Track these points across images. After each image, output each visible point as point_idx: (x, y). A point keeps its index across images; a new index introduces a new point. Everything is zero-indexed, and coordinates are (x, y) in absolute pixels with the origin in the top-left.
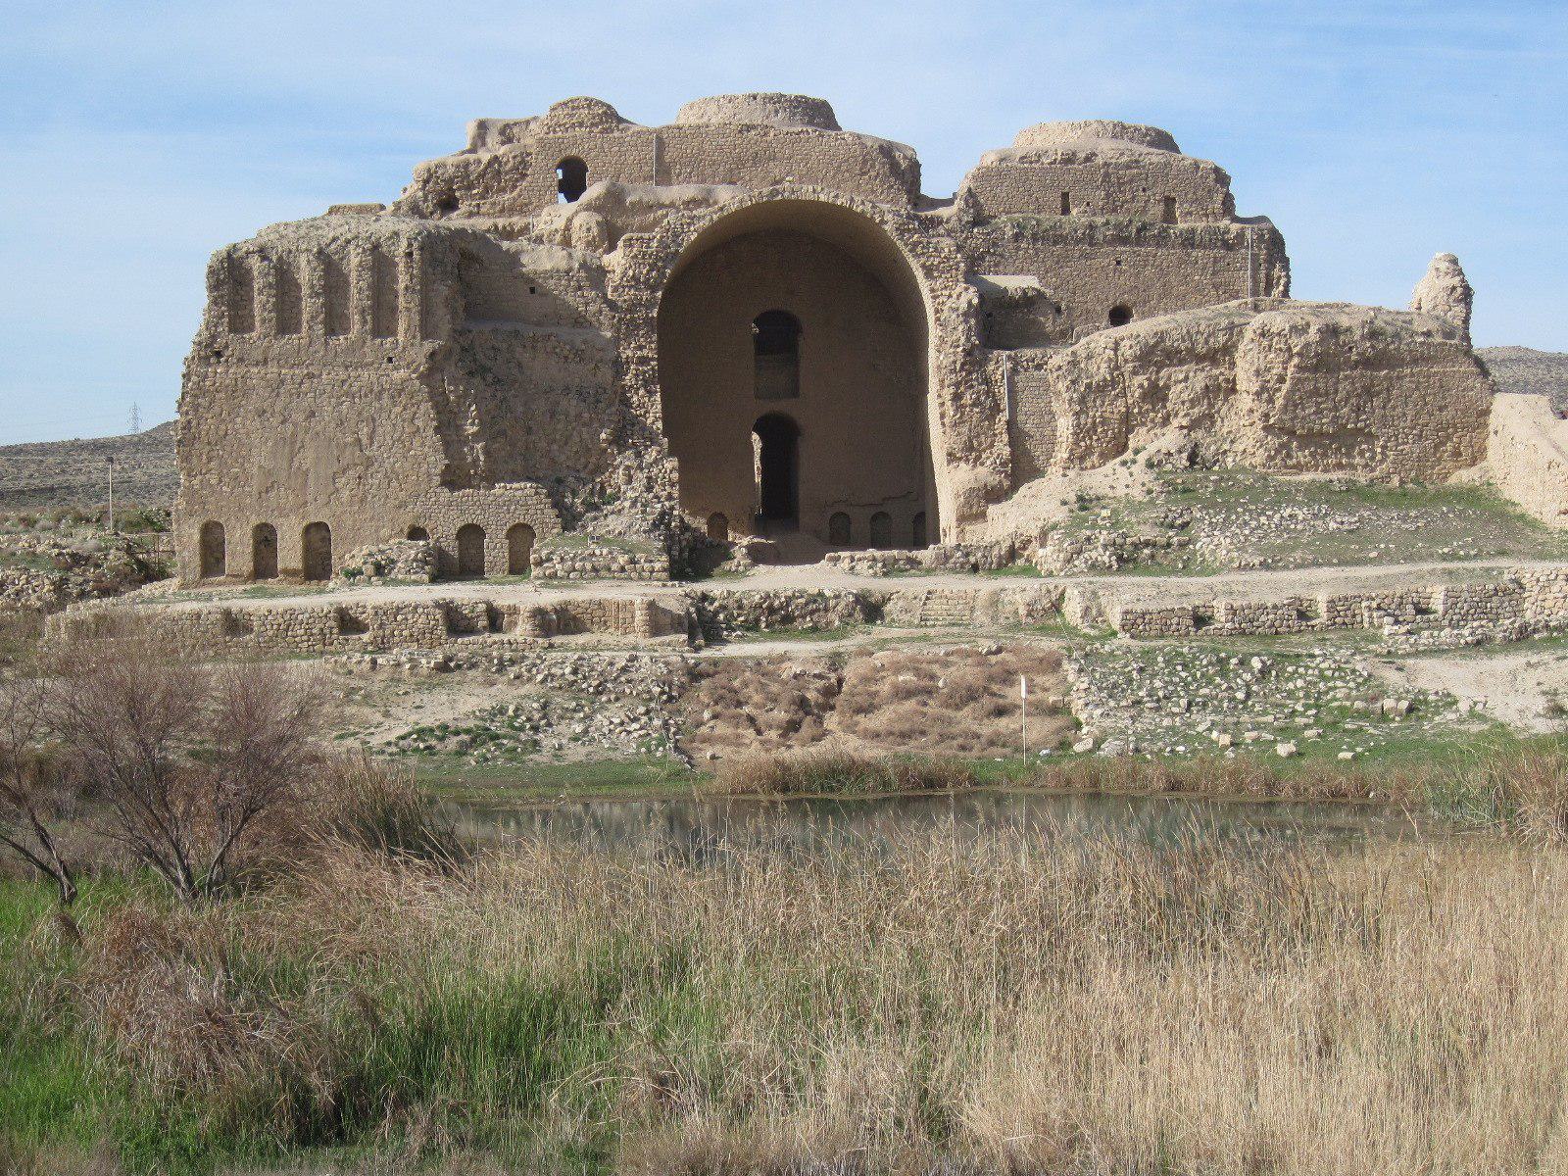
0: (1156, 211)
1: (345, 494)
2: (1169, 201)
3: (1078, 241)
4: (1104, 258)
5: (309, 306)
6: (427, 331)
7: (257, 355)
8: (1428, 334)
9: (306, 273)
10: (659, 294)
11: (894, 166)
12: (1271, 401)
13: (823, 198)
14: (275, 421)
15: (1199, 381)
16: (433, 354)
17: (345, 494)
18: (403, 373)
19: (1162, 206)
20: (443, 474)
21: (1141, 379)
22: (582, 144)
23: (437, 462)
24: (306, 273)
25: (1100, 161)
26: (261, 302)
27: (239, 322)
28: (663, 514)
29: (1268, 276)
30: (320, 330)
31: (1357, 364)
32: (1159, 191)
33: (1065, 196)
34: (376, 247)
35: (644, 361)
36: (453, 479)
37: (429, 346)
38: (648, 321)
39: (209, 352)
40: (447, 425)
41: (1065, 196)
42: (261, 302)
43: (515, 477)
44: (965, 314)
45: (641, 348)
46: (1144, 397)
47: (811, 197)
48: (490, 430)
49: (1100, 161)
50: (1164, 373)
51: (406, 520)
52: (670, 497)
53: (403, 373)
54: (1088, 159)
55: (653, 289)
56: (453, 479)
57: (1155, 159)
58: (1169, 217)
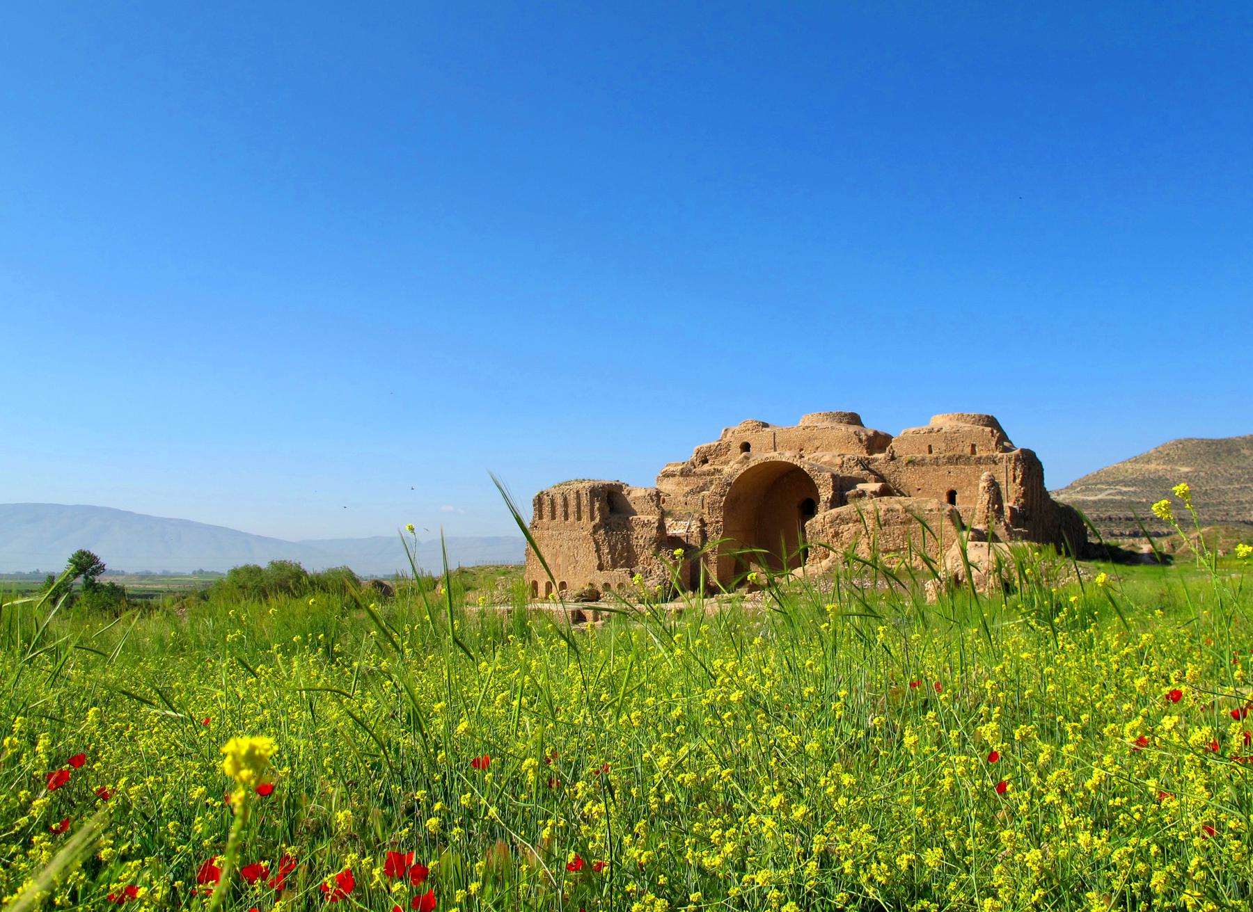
0: (968, 450)
1: (571, 572)
2: (973, 446)
3: (932, 465)
4: (943, 470)
5: (559, 510)
6: (593, 518)
7: (546, 527)
8: (931, 510)
9: (559, 501)
10: (724, 498)
11: (860, 440)
12: (869, 538)
13: (783, 460)
14: (551, 548)
15: (853, 530)
16: (594, 526)
17: (571, 572)
18: (586, 533)
19: (970, 448)
20: (598, 566)
21: (832, 530)
22: (748, 437)
23: (596, 562)
24: (559, 501)
25: (943, 431)
26: (547, 510)
27: (541, 517)
29: (1014, 475)
30: (563, 518)
31: (901, 523)
32: (968, 442)
33: (930, 446)
34: (578, 492)
35: (717, 522)
36: (601, 568)
37: (593, 523)
40: (598, 550)
41: (930, 446)
42: (547, 510)
43: (622, 566)
44: (826, 502)
45: (717, 517)
46: (833, 537)
47: (780, 460)
48: (612, 550)
49: (943, 431)
50: (841, 527)
51: (588, 581)
52: (669, 574)
53: (586, 533)
54: (938, 431)
55: (722, 496)
56: (601, 568)
57: (966, 429)
58: (973, 452)
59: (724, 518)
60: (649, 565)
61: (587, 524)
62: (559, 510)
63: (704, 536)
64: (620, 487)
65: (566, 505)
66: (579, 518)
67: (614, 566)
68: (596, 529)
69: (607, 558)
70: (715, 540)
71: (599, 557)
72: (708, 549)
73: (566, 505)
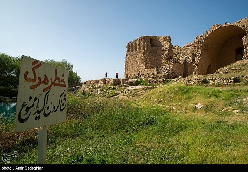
5: (134, 49)
6: (144, 48)
16: (144, 52)
23: (145, 65)
28: (169, 71)
35: (199, 53)
36: (146, 68)
37: (144, 50)
38: (200, 48)
39: (127, 55)
40: (146, 61)
52: (171, 69)
56: (146, 68)
59: (202, 52)
60: (164, 66)
61: (142, 51)
62: (134, 49)
63: (194, 60)
64: (156, 37)
65: (136, 45)
66: (140, 50)
67: (151, 67)
68: (145, 53)
69: (148, 64)
70: (197, 60)
71: (146, 64)
72: (194, 64)
73: (136, 45)
